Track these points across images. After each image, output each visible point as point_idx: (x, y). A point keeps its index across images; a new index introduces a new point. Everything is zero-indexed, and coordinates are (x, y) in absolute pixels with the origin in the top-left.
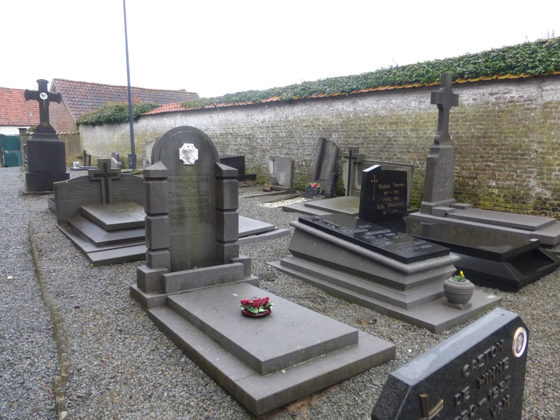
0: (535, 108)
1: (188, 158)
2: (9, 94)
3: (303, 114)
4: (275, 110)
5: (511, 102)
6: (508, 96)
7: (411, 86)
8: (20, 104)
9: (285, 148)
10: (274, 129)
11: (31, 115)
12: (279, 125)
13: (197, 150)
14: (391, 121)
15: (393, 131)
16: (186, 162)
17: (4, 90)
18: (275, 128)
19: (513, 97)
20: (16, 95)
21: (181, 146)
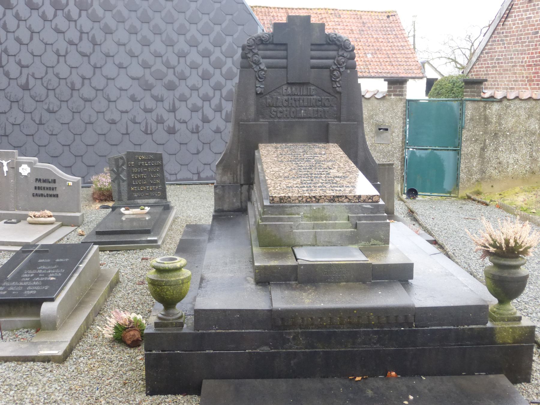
2: (336, 20)
8: (353, 36)
11: (369, 56)
17: (329, 12)
20: (347, 20)
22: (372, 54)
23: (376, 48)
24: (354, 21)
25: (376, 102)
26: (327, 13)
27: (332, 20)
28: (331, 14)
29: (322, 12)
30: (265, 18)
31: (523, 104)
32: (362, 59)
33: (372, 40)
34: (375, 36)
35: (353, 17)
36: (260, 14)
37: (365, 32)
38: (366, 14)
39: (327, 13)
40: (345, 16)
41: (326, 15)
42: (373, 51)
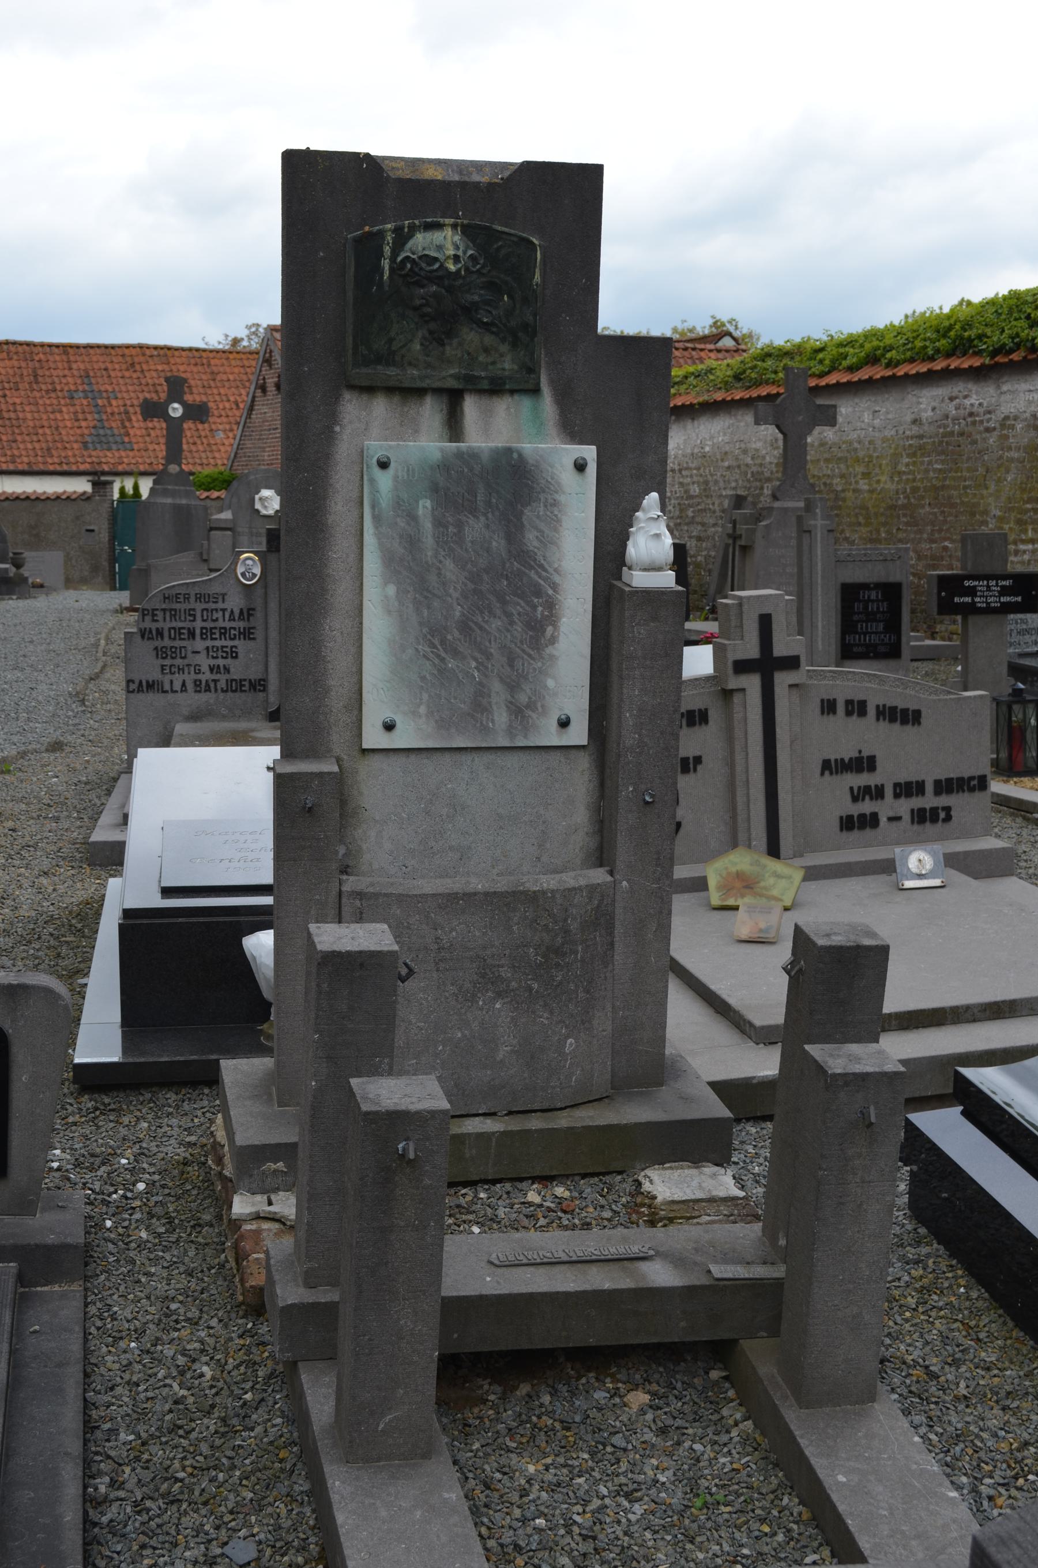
0: (994, 429)
1: (265, 507)
2: (160, 368)
3: (727, 439)
4: (685, 428)
5: (971, 414)
6: (967, 402)
7: (923, 368)
9: (698, 523)
10: (683, 476)
12: (690, 465)
13: (278, 498)
14: (839, 455)
15: (842, 476)
16: (264, 512)
18: (684, 473)
19: (972, 405)
21: (258, 492)
22: (225, 431)
23: (232, 419)
24: (195, 369)
25: (82, 503)
26: (144, 355)
27: (153, 367)
28: (151, 356)
29: (134, 352)
30: (23, 364)
31: (213, 503)
32: (205, 441)
33: (227, 405)
34: (232, 399)
35: (193, 361)
36: (15, 357)
37: (215, 391)
38: (219, 356)
39: (144, 355)
40: (178, 360)
41: (142, 359)
42: (228, 427)
